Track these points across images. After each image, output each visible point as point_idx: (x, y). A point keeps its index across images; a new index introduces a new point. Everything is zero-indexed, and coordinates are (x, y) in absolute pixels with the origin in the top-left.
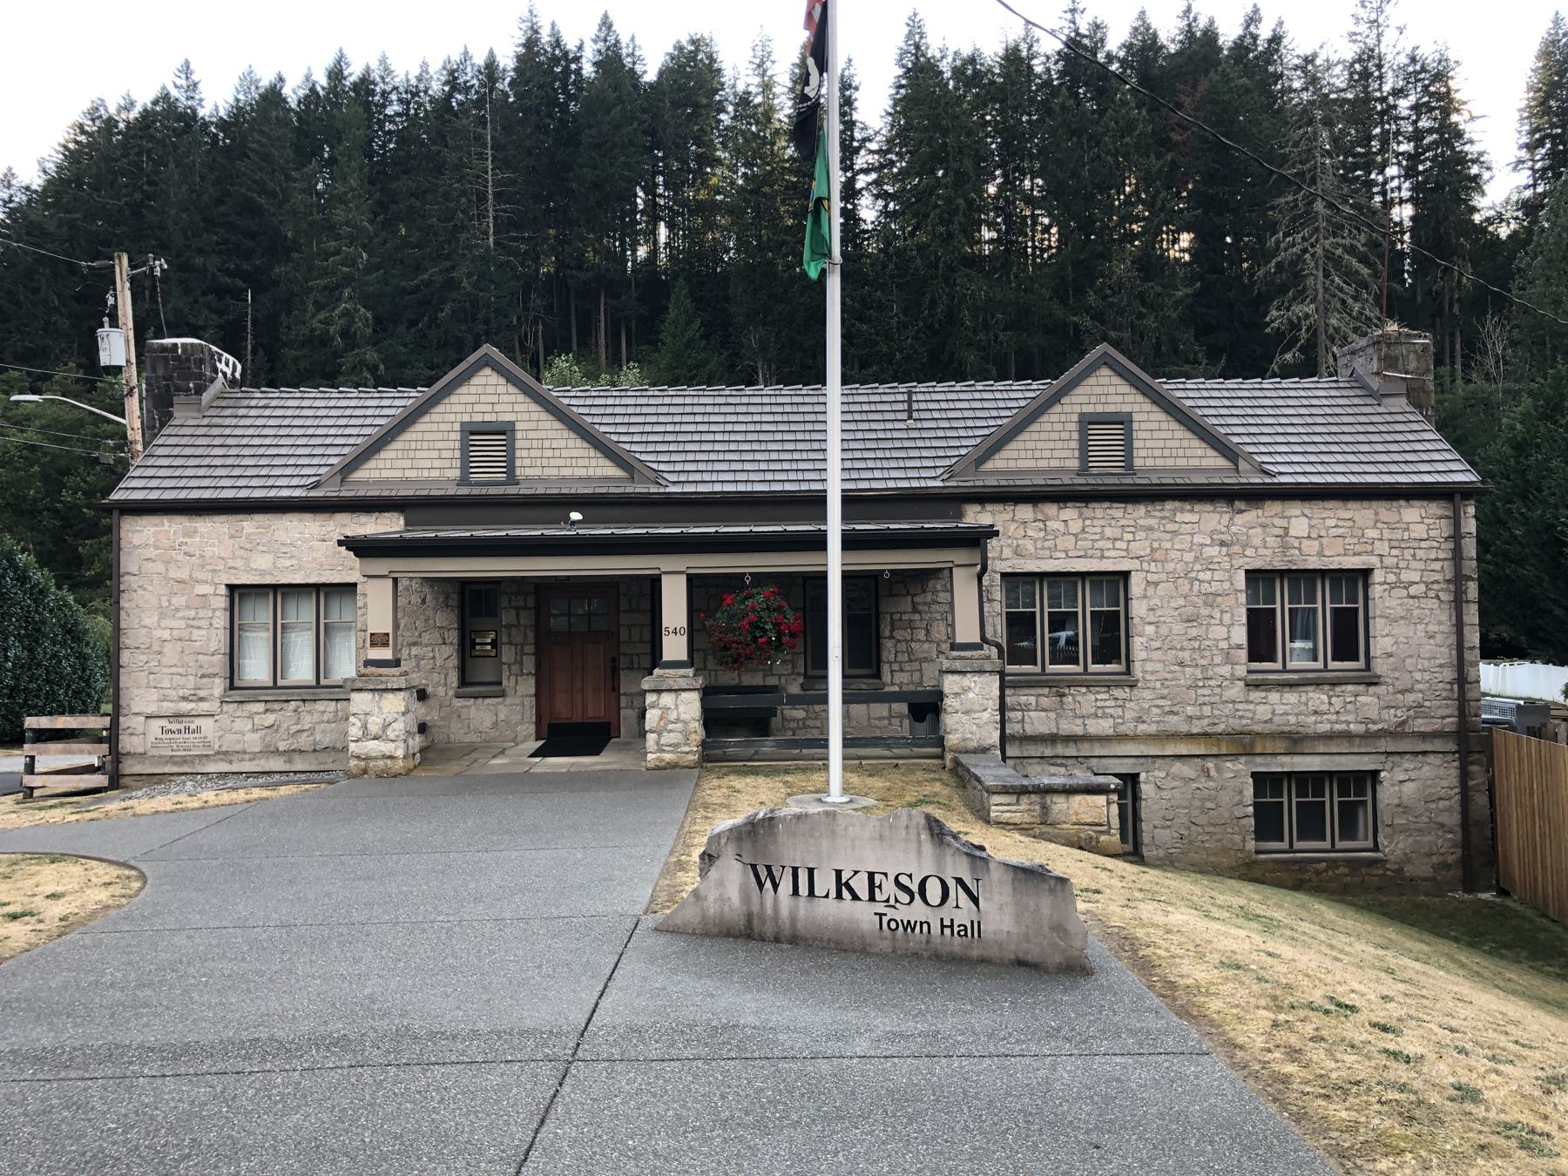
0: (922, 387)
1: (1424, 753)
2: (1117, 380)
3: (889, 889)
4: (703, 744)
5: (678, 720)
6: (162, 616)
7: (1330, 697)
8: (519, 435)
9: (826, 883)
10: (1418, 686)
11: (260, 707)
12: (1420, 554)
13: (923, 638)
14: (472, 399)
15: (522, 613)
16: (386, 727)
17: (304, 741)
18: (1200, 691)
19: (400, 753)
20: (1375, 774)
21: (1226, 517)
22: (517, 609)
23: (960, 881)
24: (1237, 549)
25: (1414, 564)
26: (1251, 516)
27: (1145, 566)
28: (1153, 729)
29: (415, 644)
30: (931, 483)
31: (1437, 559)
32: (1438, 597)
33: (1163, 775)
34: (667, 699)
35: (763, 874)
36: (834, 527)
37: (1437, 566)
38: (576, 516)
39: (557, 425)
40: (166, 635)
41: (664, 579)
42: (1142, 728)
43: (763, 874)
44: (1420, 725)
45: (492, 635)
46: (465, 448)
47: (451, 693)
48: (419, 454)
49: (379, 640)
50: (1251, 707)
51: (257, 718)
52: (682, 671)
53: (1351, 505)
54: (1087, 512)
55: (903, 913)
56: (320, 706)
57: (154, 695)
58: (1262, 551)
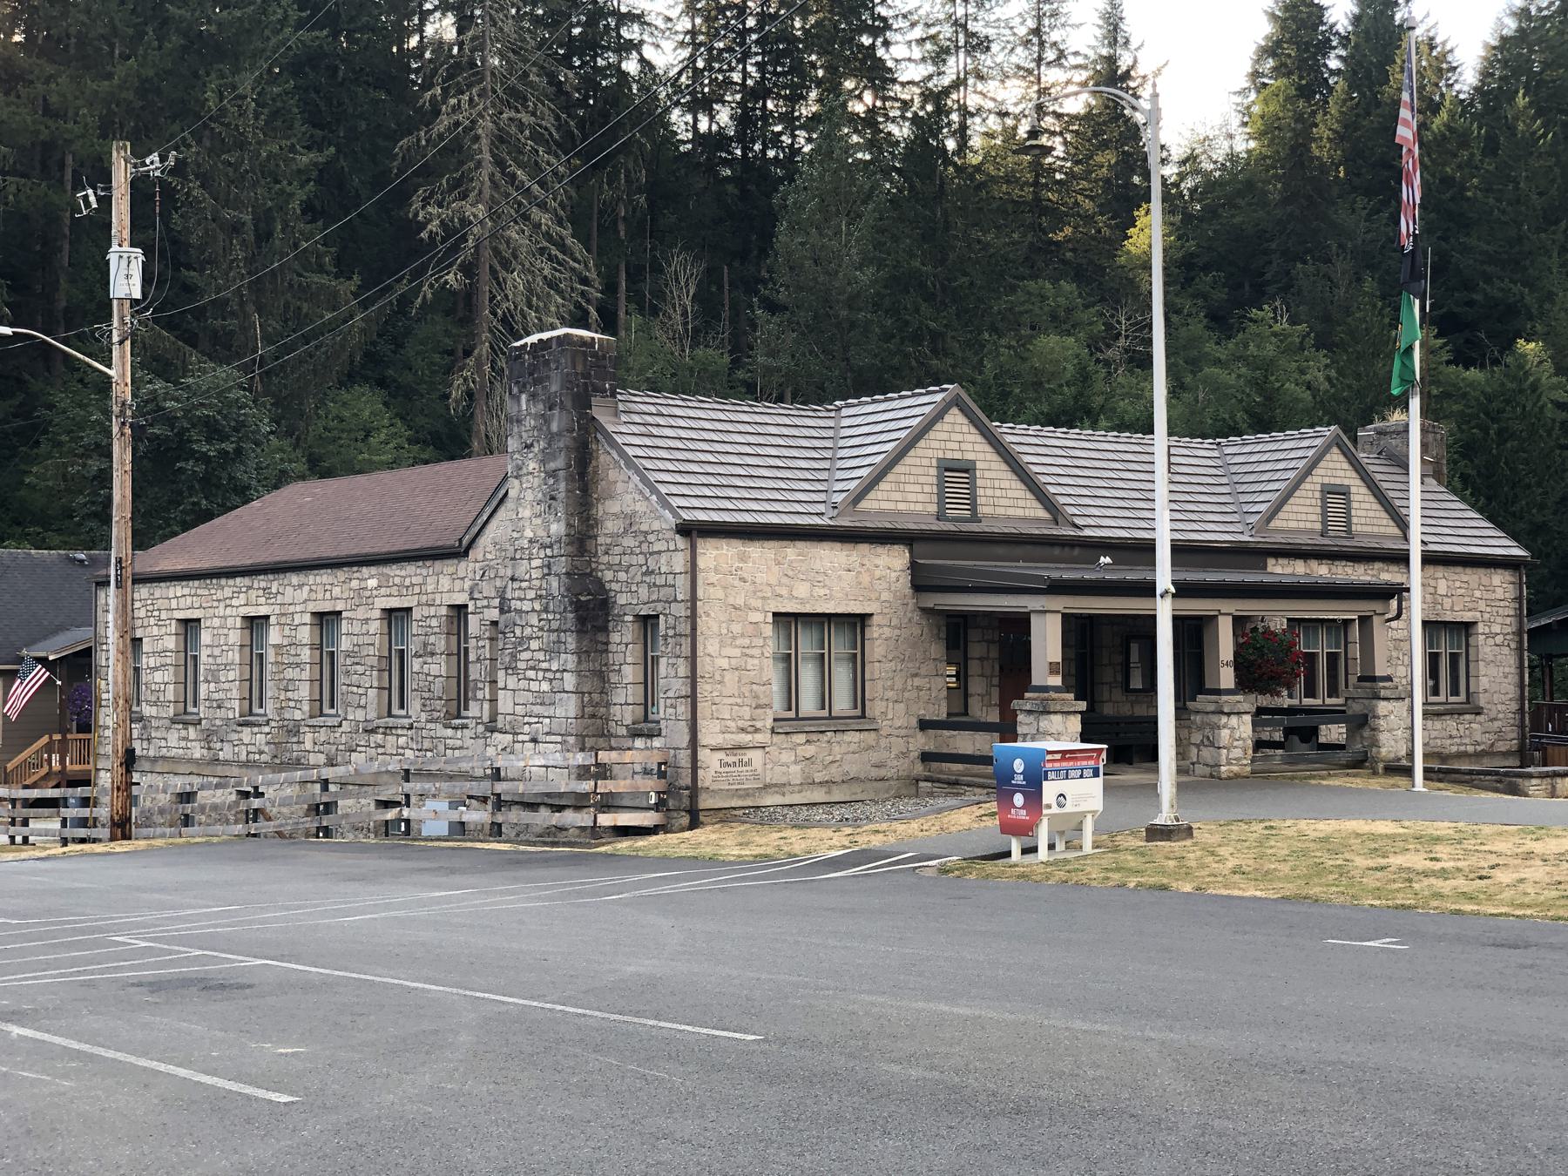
6: (722, 645)
11: (801, 738)
14: (945, 436)
17: (834, 772)
29: (916, 675)
34: (1234, 720)
36: (1164, 577)
37: (1508, 620)
39: (1004, 467)
40: (724, 663)
41: (1034, 619)
46: (941, 483)
48: (908, 488)
53: (1469, 571)
56: (848, 737)
57: (716, 726)
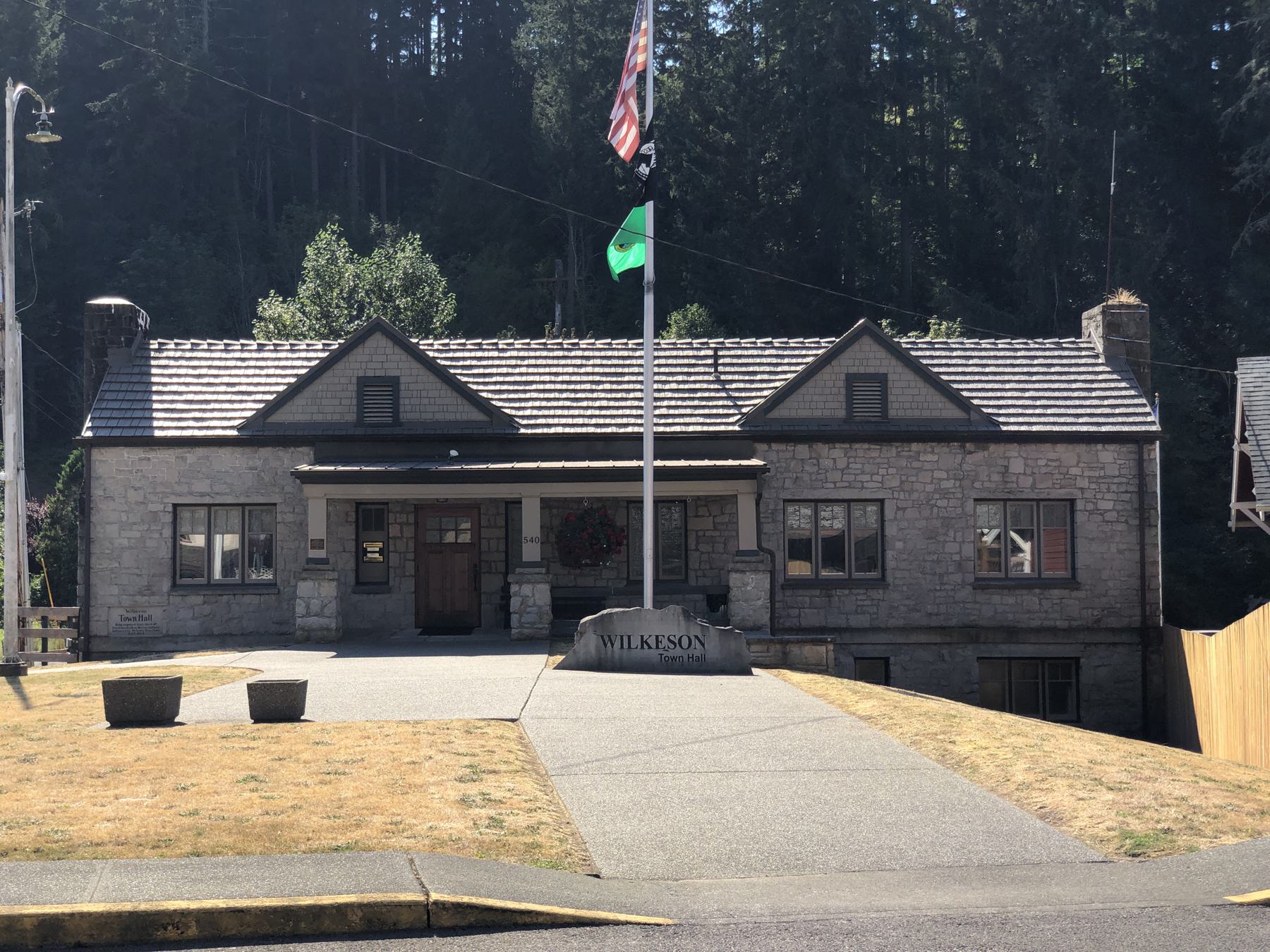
0: (728, 342)
1: (1114, 644)
2: (876, 347)
3: (665, 642)
4: (552, 623)
5: (534, 605)
7: (1040, 600)
8: (402, 387)
9: (636, 642)
10: (1110, 592)
11: (199, 599)
12: (1114, 488)
13: (721, 550)
15: (405, 528)
16: (323, 607)
18: (938, 594)
19: (333, 626)
20: (1077, 659)
21: (959, 457)
22: (401, 524)
23: (696, 637)
24: (966, 483)
25: (1108, 496)
26: (979, 456)
27: (896, 495)
28: (901, 623)
30: (730, 428)
31: (1126, 492)
32: (1126, 522)
33: (908, 658)
35: (607, 639)
37: (1126, 497)
38: (454, 453)
40: (125, 542)
42: (892, 622)
43: (607, 639)
44: (1113, 622)
45: (381, 544)
46: (361, 395)
47: (349, 590)
48: (324, 402)
49: (317, 544)
50: (977, 606)
51: (196, 609)
52: (537, 570)
54: (852, 453)
55: (671, 653)
58: (987, 485)
